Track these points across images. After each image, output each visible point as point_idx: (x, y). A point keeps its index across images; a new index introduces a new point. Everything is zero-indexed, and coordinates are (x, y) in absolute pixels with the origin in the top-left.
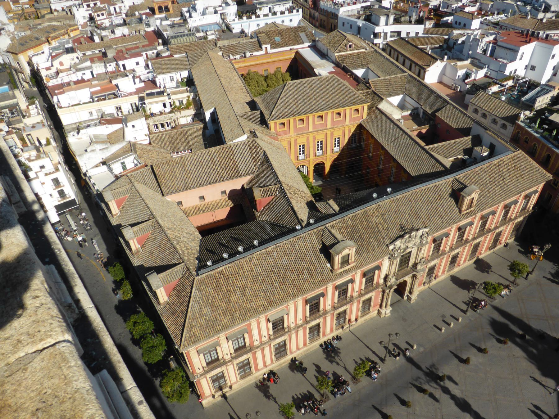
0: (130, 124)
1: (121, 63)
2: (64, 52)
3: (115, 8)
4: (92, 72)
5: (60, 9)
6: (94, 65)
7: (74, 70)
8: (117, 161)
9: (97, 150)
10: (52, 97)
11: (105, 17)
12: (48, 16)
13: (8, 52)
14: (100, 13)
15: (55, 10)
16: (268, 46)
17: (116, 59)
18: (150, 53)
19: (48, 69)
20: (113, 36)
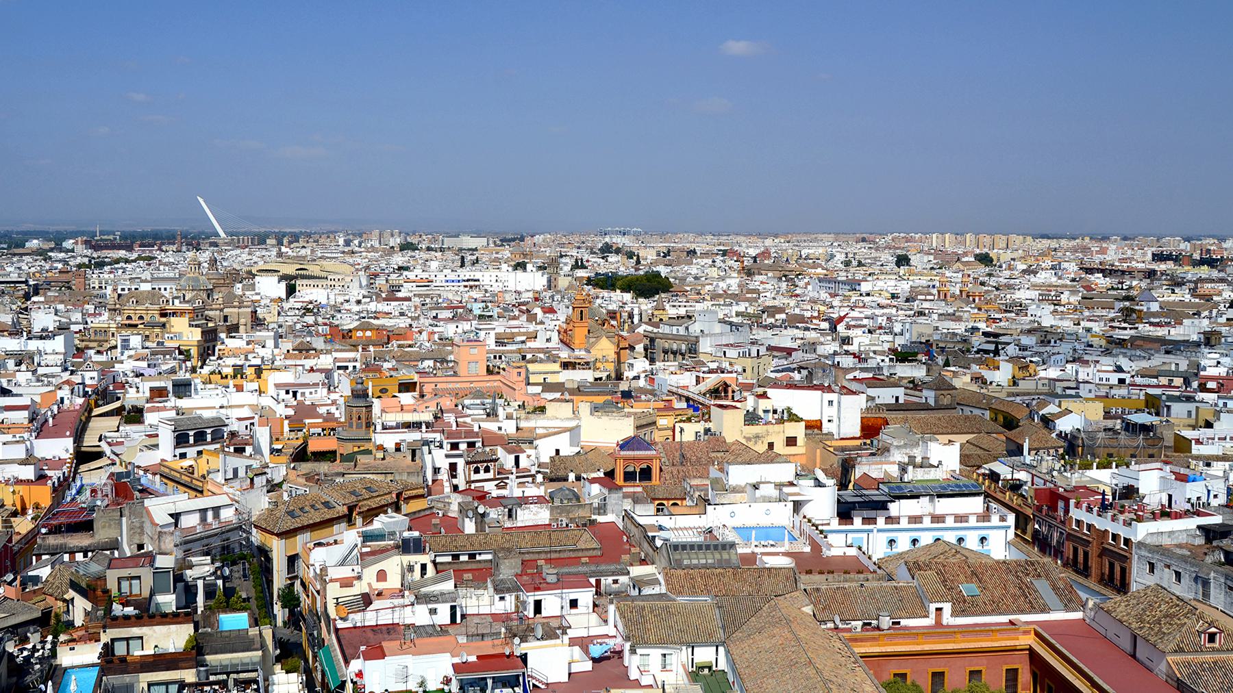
1: (531, 599)
2: (397, 547)
3: (517, 458)
4: (453, 608)
7: (413, 598)
10: (347, 662)
11: (490, 475)
12: (362, 459)
14: (482, 467)
15: (380, 447)
16: (947, 607)
18: (607, 581)
19: (346, 583)
20: (508, 524)
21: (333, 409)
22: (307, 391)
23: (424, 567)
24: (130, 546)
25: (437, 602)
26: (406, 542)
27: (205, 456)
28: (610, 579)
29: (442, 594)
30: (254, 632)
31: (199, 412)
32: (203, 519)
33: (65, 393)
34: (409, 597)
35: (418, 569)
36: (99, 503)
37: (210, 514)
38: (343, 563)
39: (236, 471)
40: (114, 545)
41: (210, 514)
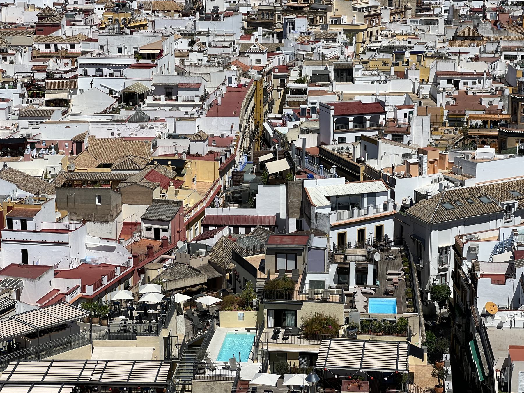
21: (496, 101)
22: (470, 82)
31: (357, 98)
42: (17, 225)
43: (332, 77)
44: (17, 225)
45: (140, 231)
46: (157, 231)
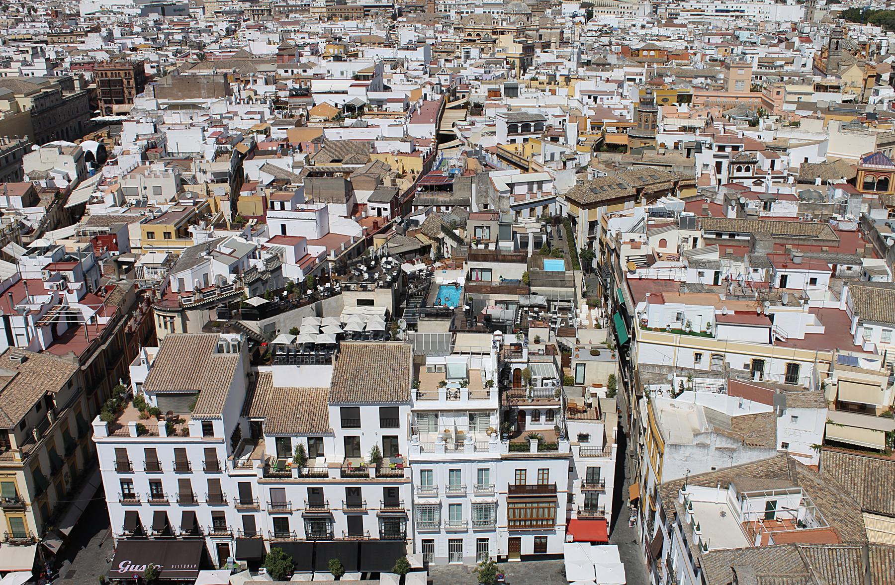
0: (789, 412)
3: (773, 163)
5: (670, 144)
6: (724, 262)
8: (762, 495)
9: (712, 448)
11: (750, 174)
13: (568, 199)
15: (663, 145)
17: (769, 263)
20: (763, 214)
21: (625, 113)
22: (605, 97)
23: (695, 240)
24: (478, 204)
25: (705, 267)
26: (683, 220)
27: (530, 143)
28: (845, 267)
29: (709, 262)
30: (569, 273)
31: (523, 110)
32: (530, 189)
33: (427, 90)
34: (683, 262)
35: (691, 241)
36: (457, 172)
37: (535, 186)
38: (632, 231)
39: (553, 155)
40: (467, 203)
41: (535, 186)
42: (277, 205)
43: (502, 91)
44: (277, 205)
45: (366, 212)
46: (379, 210)
